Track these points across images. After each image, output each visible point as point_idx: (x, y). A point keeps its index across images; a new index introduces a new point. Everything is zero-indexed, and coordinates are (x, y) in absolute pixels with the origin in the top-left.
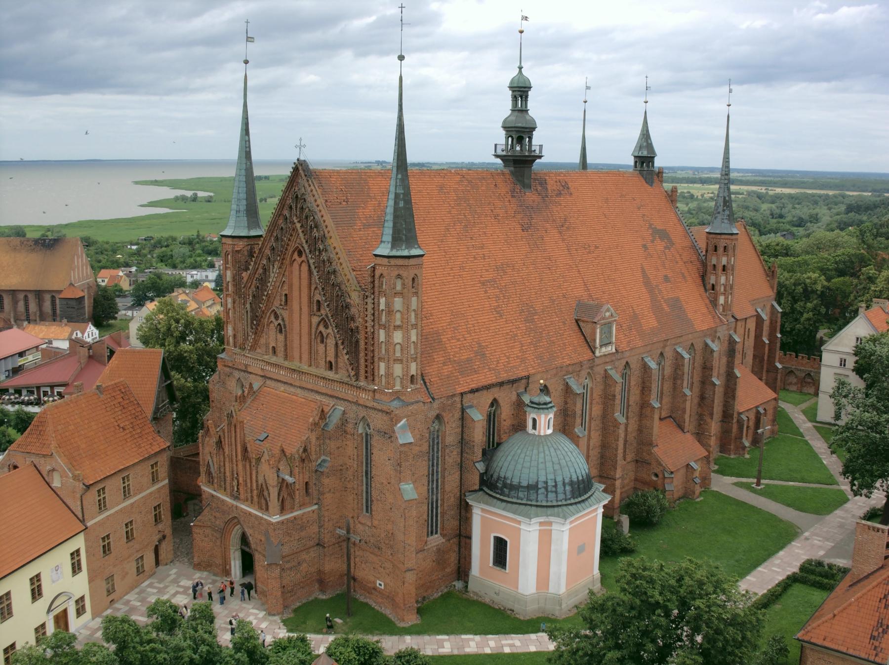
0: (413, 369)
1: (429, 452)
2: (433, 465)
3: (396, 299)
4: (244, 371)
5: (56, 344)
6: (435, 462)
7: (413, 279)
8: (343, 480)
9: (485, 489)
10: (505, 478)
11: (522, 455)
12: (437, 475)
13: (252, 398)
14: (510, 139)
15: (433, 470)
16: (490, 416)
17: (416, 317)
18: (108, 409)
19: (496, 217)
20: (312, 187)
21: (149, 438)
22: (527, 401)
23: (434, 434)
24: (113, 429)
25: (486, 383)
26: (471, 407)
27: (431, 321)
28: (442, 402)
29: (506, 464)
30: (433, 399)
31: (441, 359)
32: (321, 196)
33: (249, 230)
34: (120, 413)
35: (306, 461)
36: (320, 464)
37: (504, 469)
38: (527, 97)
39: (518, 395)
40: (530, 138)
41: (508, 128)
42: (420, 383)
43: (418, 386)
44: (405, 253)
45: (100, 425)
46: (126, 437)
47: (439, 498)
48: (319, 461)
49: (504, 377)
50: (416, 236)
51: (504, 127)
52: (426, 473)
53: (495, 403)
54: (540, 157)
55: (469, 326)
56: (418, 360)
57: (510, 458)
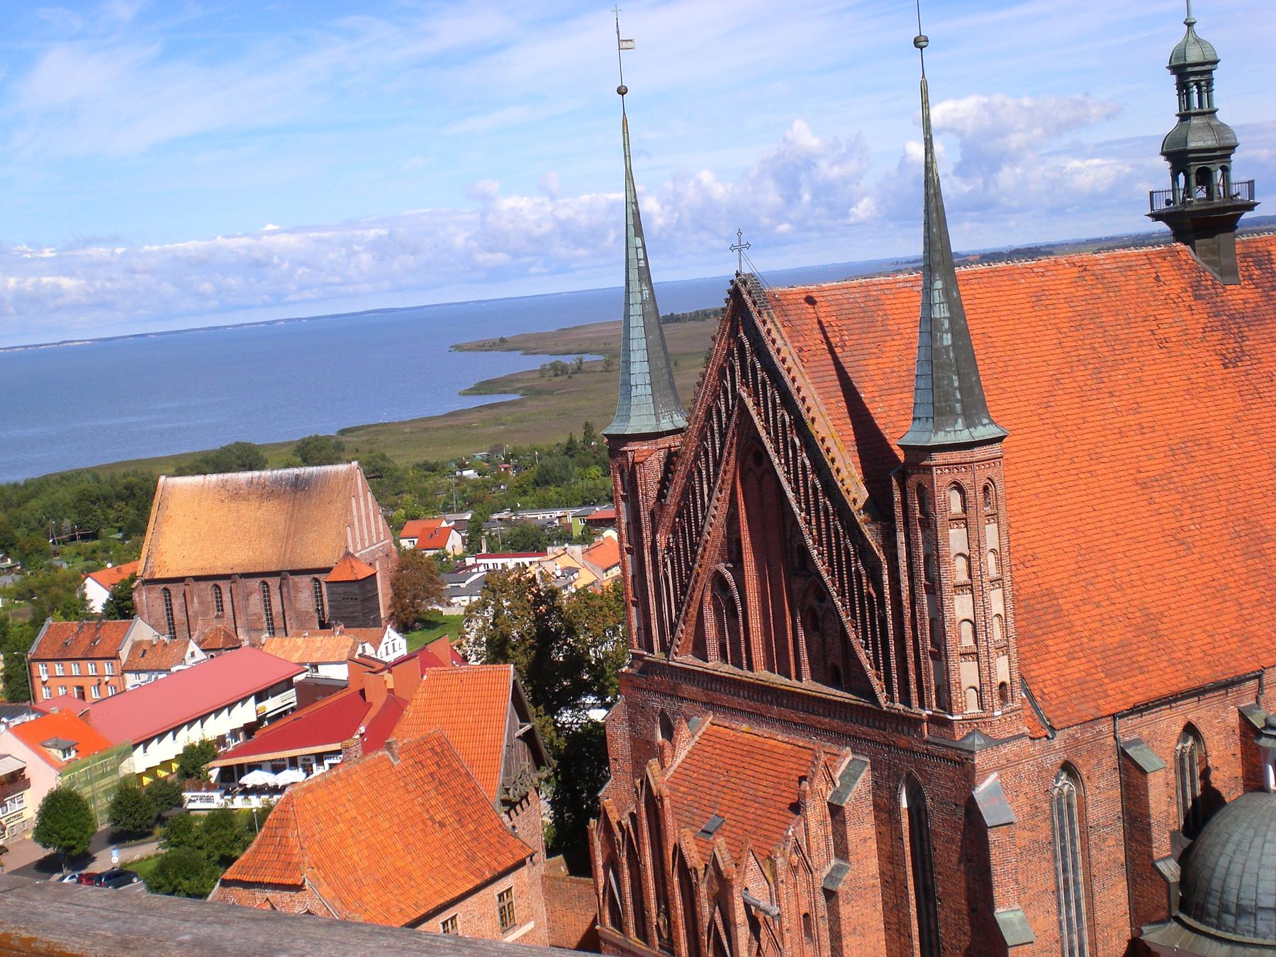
0: (1002, 670)
1: (1051, 843)
2: (1065, 870)
3: (951, 531)
4: (671, 696)
5: (325, 672)
6: (1069, 861)
7: (986, 489)
8: (880, 906)
9: (1183, 916)
10: (1223, 892)
11: (1258, 841)
12: (1077, 891)
13: (689, 748)
14: (1182, 177)
15: (1066, 881)
16: (1182, 759)
17: (999, 564)
18: (411, 787)
19: (1163, 343)
20: (769, 325)
21: (492, 841)
22: (1259, 724)
23: (1059, 803)
24: (421, 827)
25: (1165, 692)
26: (1137, 742)
27: (1034, 569)
28: (1072, 736)
29: (1223, 862)
30: (1052, 728)
31: (1067, 645)
32: (787, 339)
33: (658, 420)
34: (433, 793)
35: (801, 871)
36: (829, 876)
37: (1219, 873)
38: (1209, 83)
39: (1242, 715)
40: (1225, 170)
41: (1178, 157)
42: (1020, 695)
43: (1017, 705)
44: (964, 437)
45: (396, 820)
46: (446, 841)
47: (1086, 940)
48: (828, 869)
49: (1205, 675)
50: (984, 402)
51: (1168, 155)
52: (1050, 884)
53: (1190, 730)
54: (1250, 207)
55: (1117, 575)
56: (1013, 651)
57: (1230, 848)
